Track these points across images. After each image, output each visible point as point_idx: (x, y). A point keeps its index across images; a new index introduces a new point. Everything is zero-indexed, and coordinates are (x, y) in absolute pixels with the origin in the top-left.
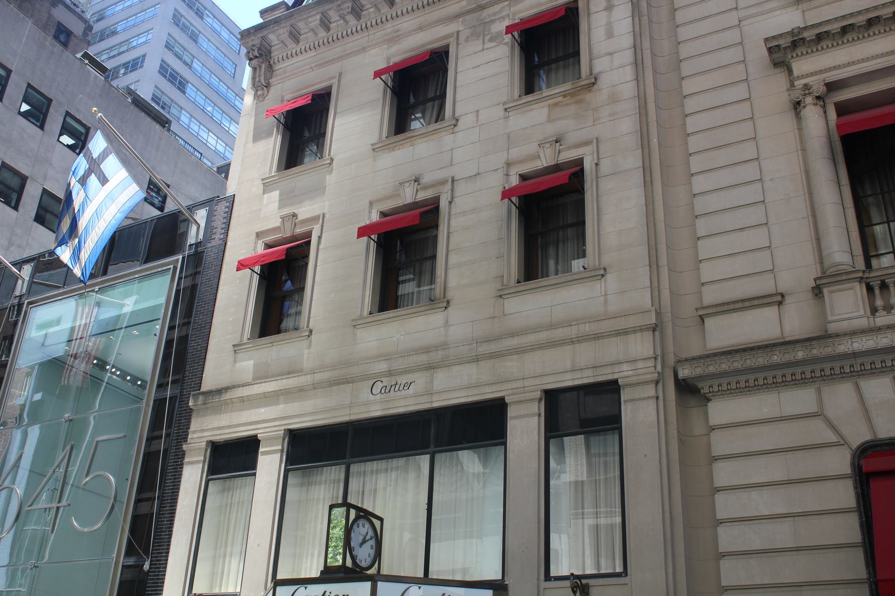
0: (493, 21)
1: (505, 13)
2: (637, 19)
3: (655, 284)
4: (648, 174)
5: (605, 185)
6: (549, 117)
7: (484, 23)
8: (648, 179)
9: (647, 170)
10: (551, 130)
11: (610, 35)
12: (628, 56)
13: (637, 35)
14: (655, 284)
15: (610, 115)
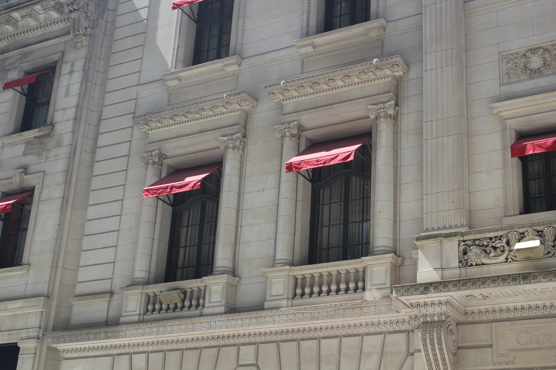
0: (9, 70)
1: (16, 65)
2: (84, 84)
3: (52, 280)
4: (65, 202)
5: (43, 207)
6: (24, 152)
7: (5, 70)
8: (64, 205)
9: (65, 199)
10: (24, 161)
11: (67, 95)
12: (71, 113)
13: (83, 95)
14: (52, 280)
15: (56, 156)
